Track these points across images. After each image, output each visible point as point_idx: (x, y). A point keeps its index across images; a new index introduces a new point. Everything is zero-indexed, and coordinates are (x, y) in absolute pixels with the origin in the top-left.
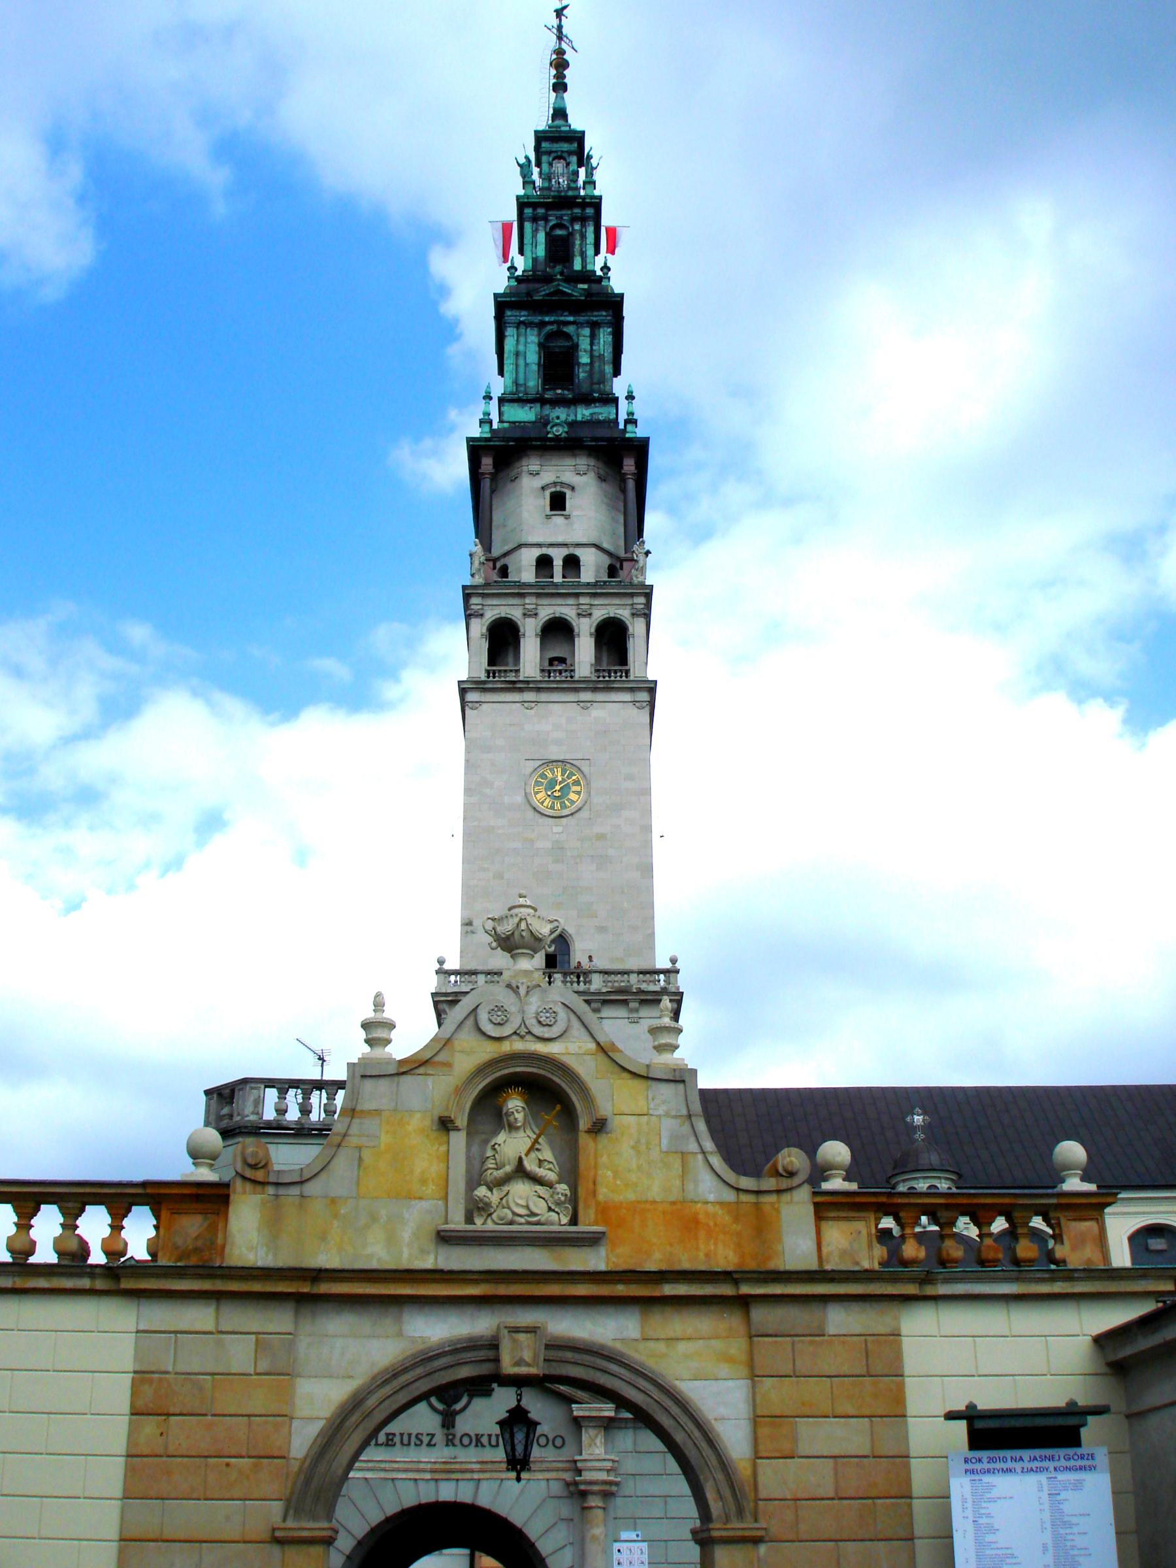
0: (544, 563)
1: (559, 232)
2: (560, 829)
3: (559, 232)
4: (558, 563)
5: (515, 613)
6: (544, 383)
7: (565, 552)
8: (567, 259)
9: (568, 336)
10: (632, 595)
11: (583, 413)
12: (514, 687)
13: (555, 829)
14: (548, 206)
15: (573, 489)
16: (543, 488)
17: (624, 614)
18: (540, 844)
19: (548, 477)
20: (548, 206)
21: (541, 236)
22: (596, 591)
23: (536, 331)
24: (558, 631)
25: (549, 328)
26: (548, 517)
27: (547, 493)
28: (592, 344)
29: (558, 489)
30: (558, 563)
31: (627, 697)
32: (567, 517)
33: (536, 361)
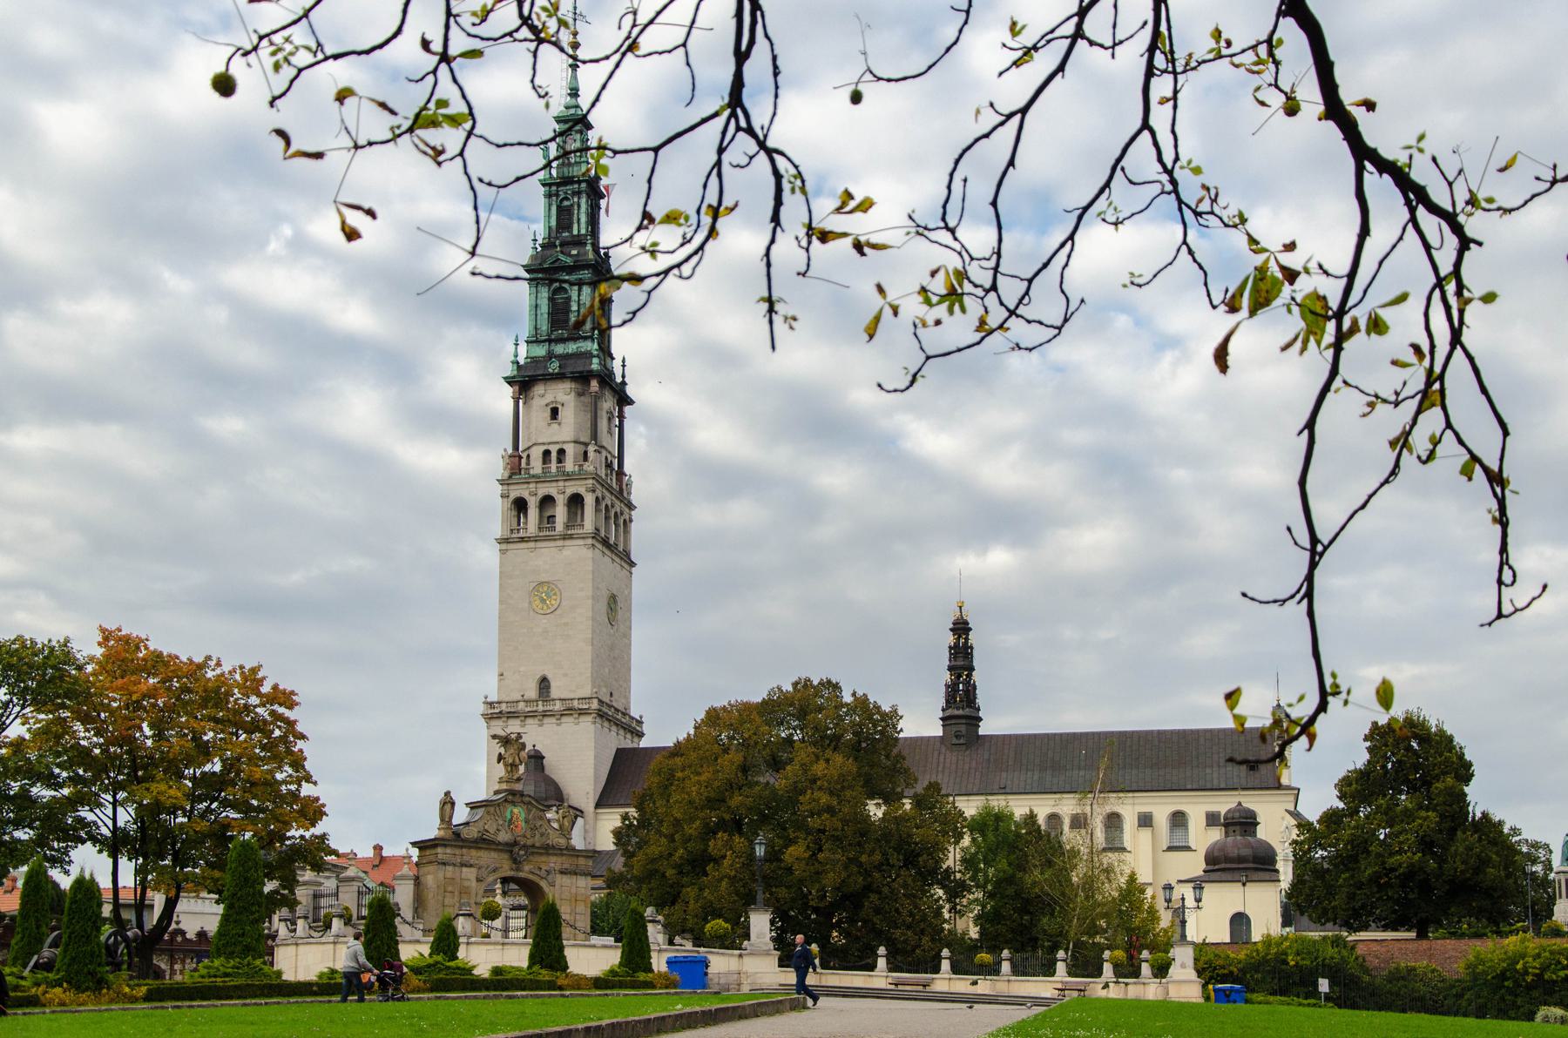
0: (547, 453)
1: (566, 203)
3: (566, 203)
4: (554, 455)
5: (525, 495)
7: (558, 447)
8: (569, 227)
11: (572, 347)
12: (522, 540)
14: (558, 185)
17: (582, 491)
19: (549, 398)
20: (558, 185)
21: (554, 208)
22: (569, 477)
24: (547, 501)
30: (554, 455)
31: (581, 542)
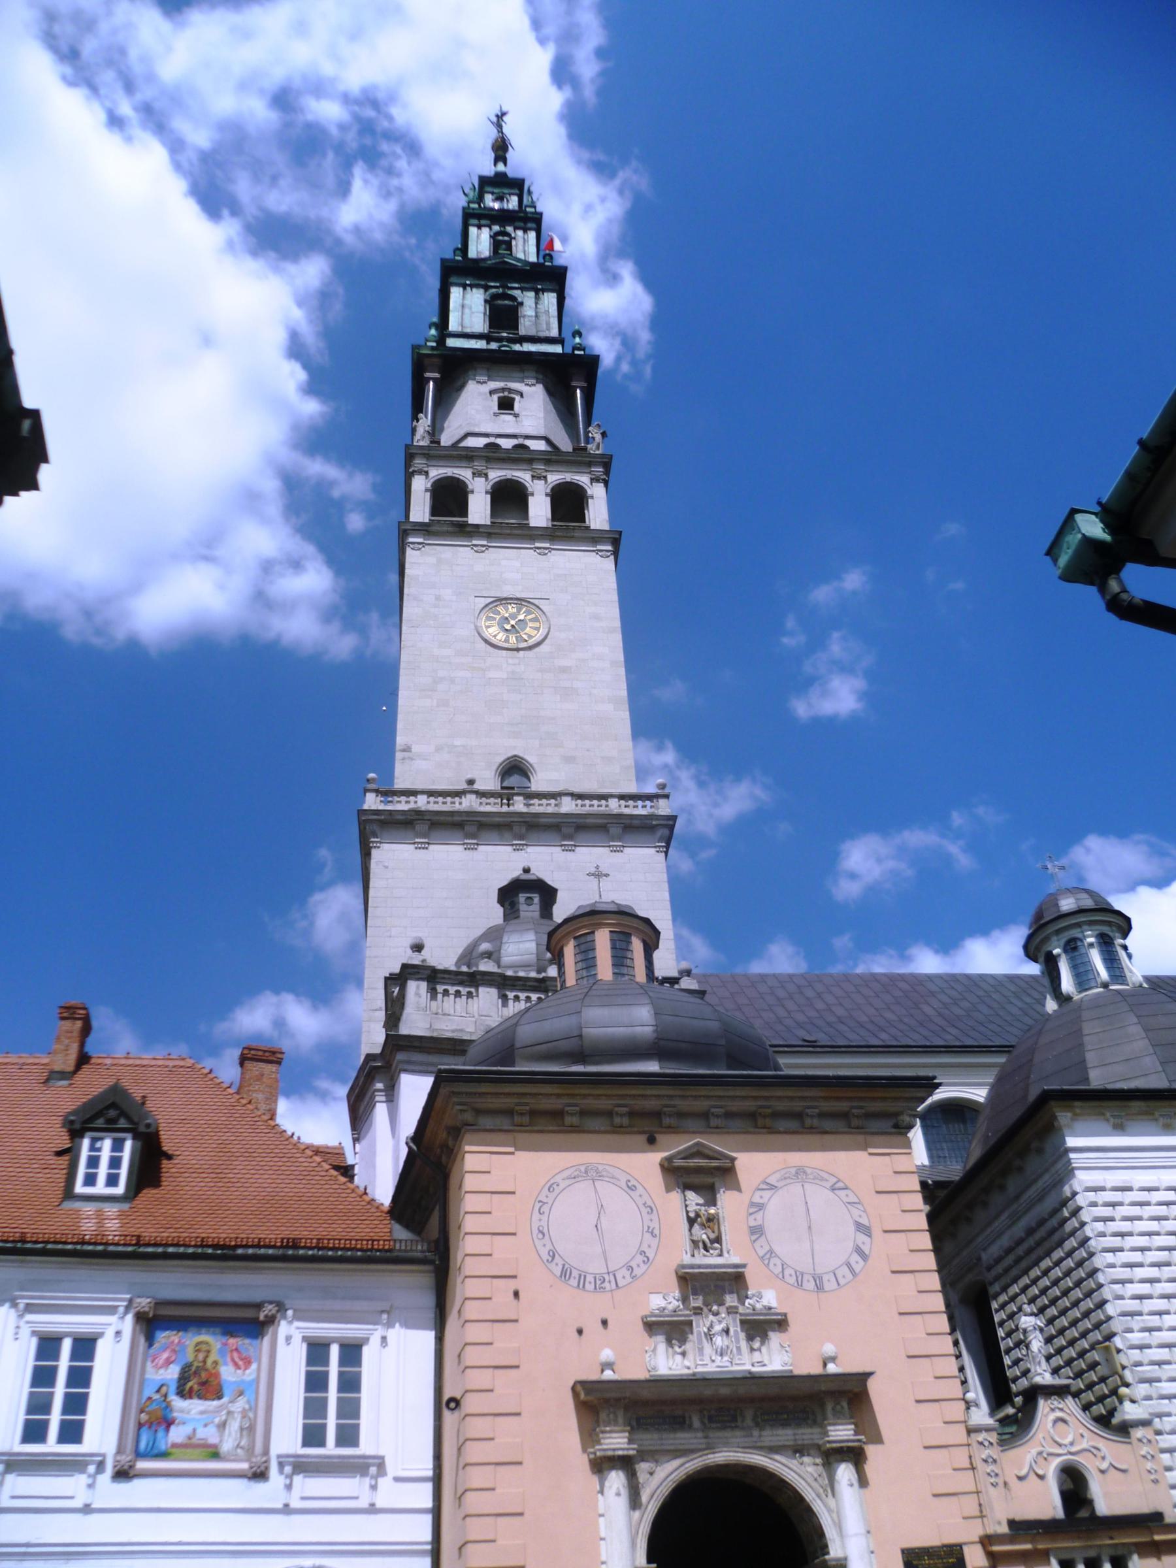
2: (516, 661)
6: (490, 327)
9: (514, 298)
10: (590, 464)
12: (466, 531)
13: (510, 661)
15: (522, 396)
16: (491, 392)
18: (492, 674)
23: (482, 291)
25: (494, 290)
26: (496, 415)
27: (495, 397)
28: (536, 304)
29: (506, 394)
32: (516, 416)
33: (482, 309)
